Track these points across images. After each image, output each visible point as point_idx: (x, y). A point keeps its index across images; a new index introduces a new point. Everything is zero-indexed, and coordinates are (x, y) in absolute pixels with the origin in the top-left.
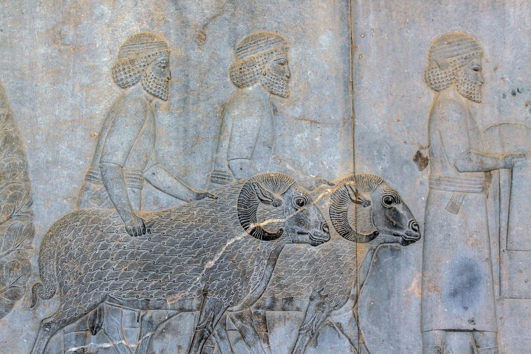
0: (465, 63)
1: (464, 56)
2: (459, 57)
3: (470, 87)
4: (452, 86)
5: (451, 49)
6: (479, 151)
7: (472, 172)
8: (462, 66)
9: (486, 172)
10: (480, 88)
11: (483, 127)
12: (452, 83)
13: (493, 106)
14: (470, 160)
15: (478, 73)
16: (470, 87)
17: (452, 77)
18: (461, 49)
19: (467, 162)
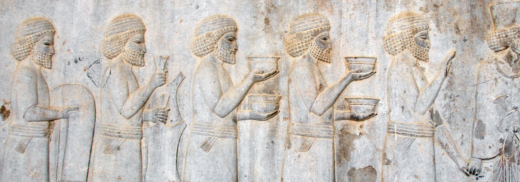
0: (38, 39)
1: (37, 34)
2: (33, 35)
3: (41, 57)
4: (29, 56)
5: (29, 29)
6: (45, 106)
7: (37, 121)
8: (37, 41)
9: (50, 121)
10: (51, 58)
11: (51, 88)
12: (29, 54)
13: (60, 71)
14: (34, 112)
15: (51, 47)
16: (41, 57)
17: (29, 50)
18: (36, 29)
19: (33, 114)
